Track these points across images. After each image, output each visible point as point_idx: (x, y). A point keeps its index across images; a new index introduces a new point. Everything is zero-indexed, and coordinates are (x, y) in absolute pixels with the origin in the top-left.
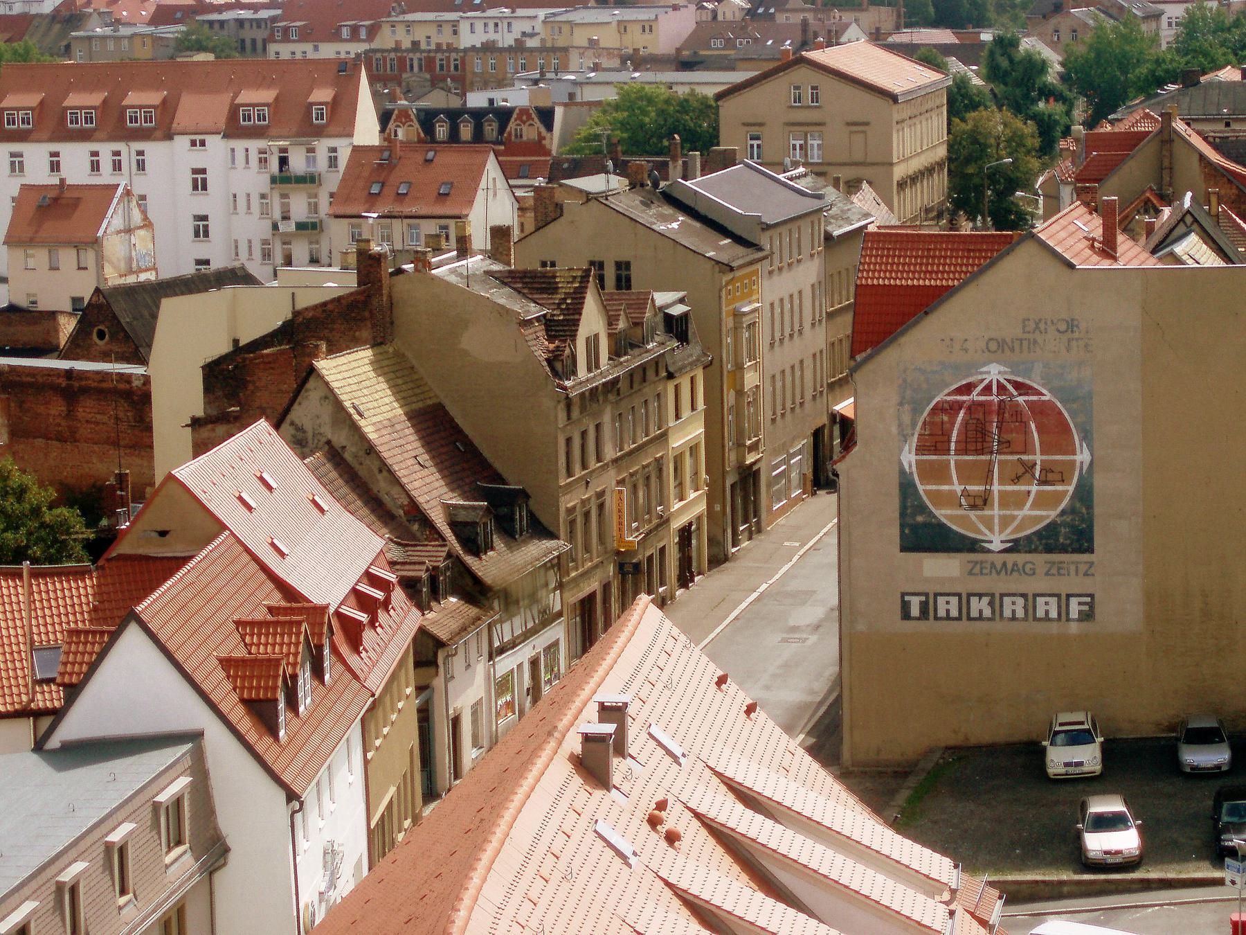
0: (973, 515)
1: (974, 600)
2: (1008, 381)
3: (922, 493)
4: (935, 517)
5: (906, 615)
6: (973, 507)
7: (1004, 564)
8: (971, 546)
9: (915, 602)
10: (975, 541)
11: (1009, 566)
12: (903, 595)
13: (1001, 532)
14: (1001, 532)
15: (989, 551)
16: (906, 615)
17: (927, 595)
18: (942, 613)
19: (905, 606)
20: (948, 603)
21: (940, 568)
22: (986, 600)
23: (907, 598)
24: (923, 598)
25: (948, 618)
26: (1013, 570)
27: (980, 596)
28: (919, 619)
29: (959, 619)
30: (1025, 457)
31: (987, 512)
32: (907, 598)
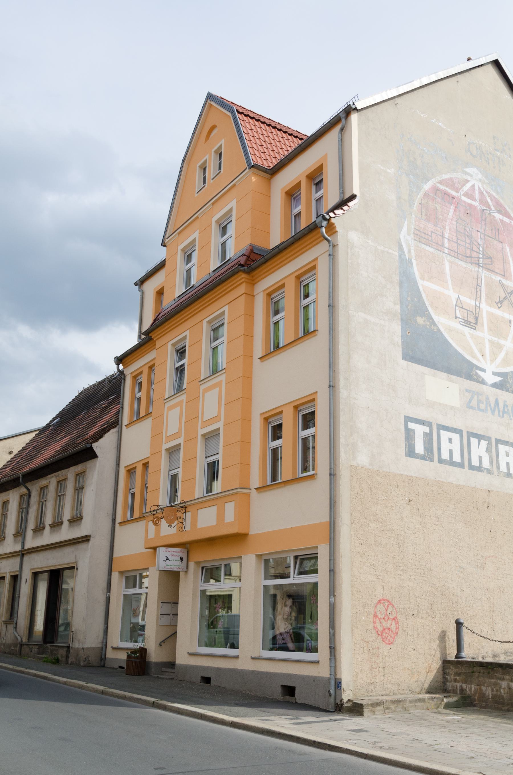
0: (466, 330)
1: (474, 441)
2: (487, 192)
3: (421, 288)
4: (433, 323)
5: (411, 452)
6: (467, 323)
7: (497, 402)
8: (466, 371)
9: (419, 430)
10: (472, 366)
11: (501, 405)
12: (408, 419)
13: (492, 361)
14: (492, 361)
15: (482, 382)
16: (411, 452)
17: (430, 425)
18: (445, 455)
19: (409, 435)
20: (450, 441)
21: (441, 391)
22: (484, 444)
23: (412, 425)
24: (427, 429)
25: (452, 463)
26: (504, 412)
27: (480, 437)
28: (422, 458)
29: (461, 465)
30: (504, 281)
31: (478, 333)
32: (412, 425)
